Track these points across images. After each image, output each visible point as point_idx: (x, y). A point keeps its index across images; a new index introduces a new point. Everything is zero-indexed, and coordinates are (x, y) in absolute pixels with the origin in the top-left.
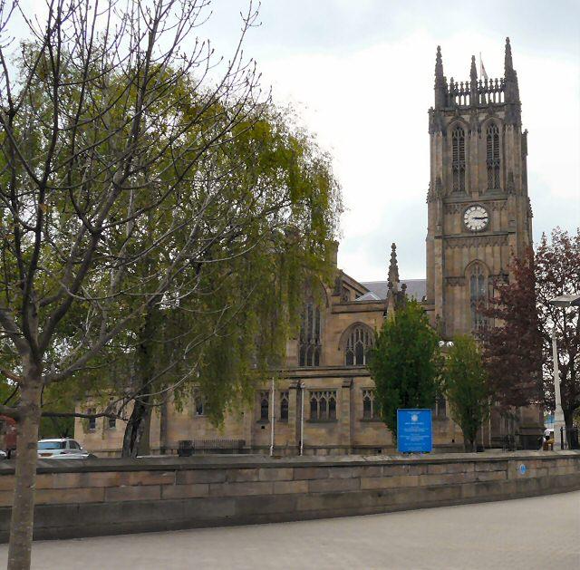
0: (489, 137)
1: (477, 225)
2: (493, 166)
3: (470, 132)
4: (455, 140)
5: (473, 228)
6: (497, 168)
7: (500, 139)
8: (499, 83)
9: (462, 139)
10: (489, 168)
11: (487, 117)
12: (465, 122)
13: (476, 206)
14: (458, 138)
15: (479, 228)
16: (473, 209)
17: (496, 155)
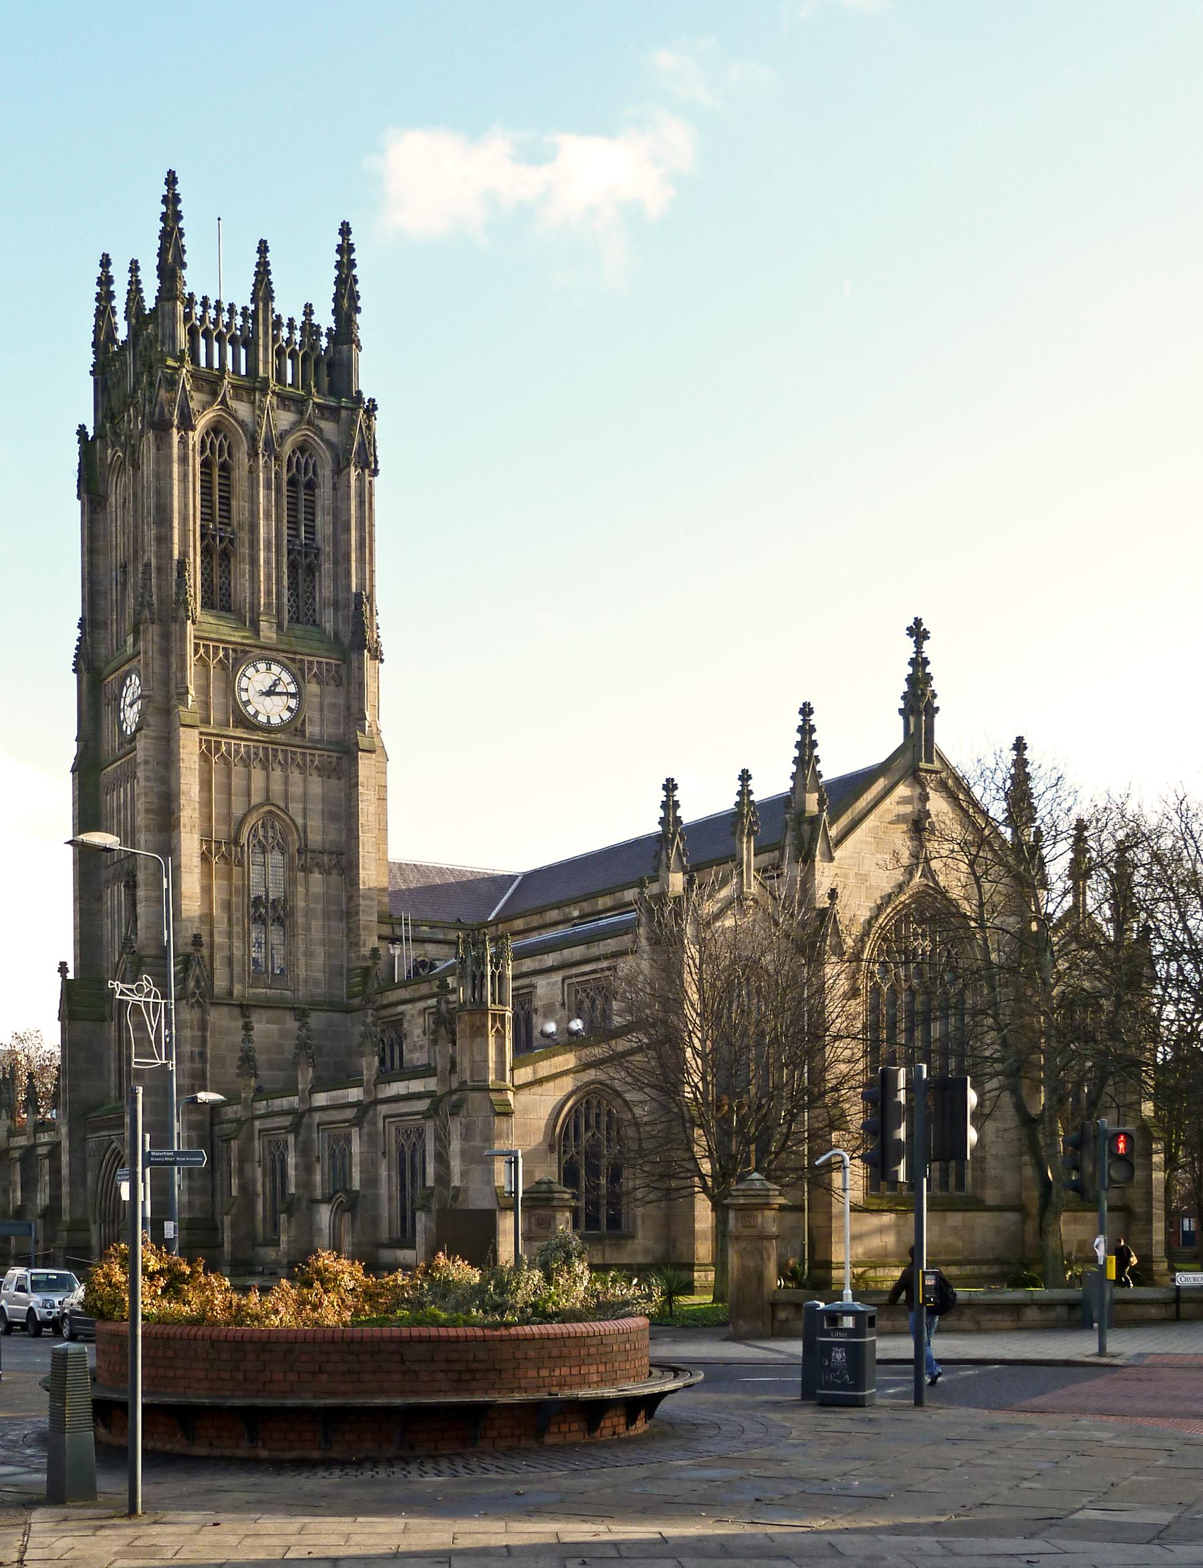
0: (292, 482)
1: (274, 711)
2: (304, 562)
3: (253, 454)
4: (206, 464)
5: (262, 718)
6: (311, 570)
7: (324, 494)
8: (324, 342)
9: (224, 467)
10: (293, 566)
11: (295, 426)
12: (242, 424)
13: (269, 661)
14: (217, 461)
15: (275, 720)
16: (262, 666)
17: (311, 530)
